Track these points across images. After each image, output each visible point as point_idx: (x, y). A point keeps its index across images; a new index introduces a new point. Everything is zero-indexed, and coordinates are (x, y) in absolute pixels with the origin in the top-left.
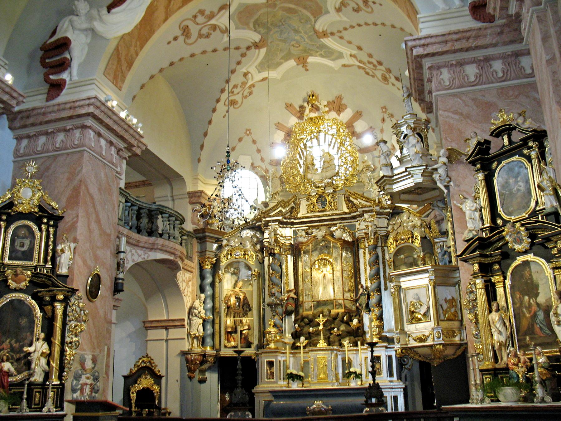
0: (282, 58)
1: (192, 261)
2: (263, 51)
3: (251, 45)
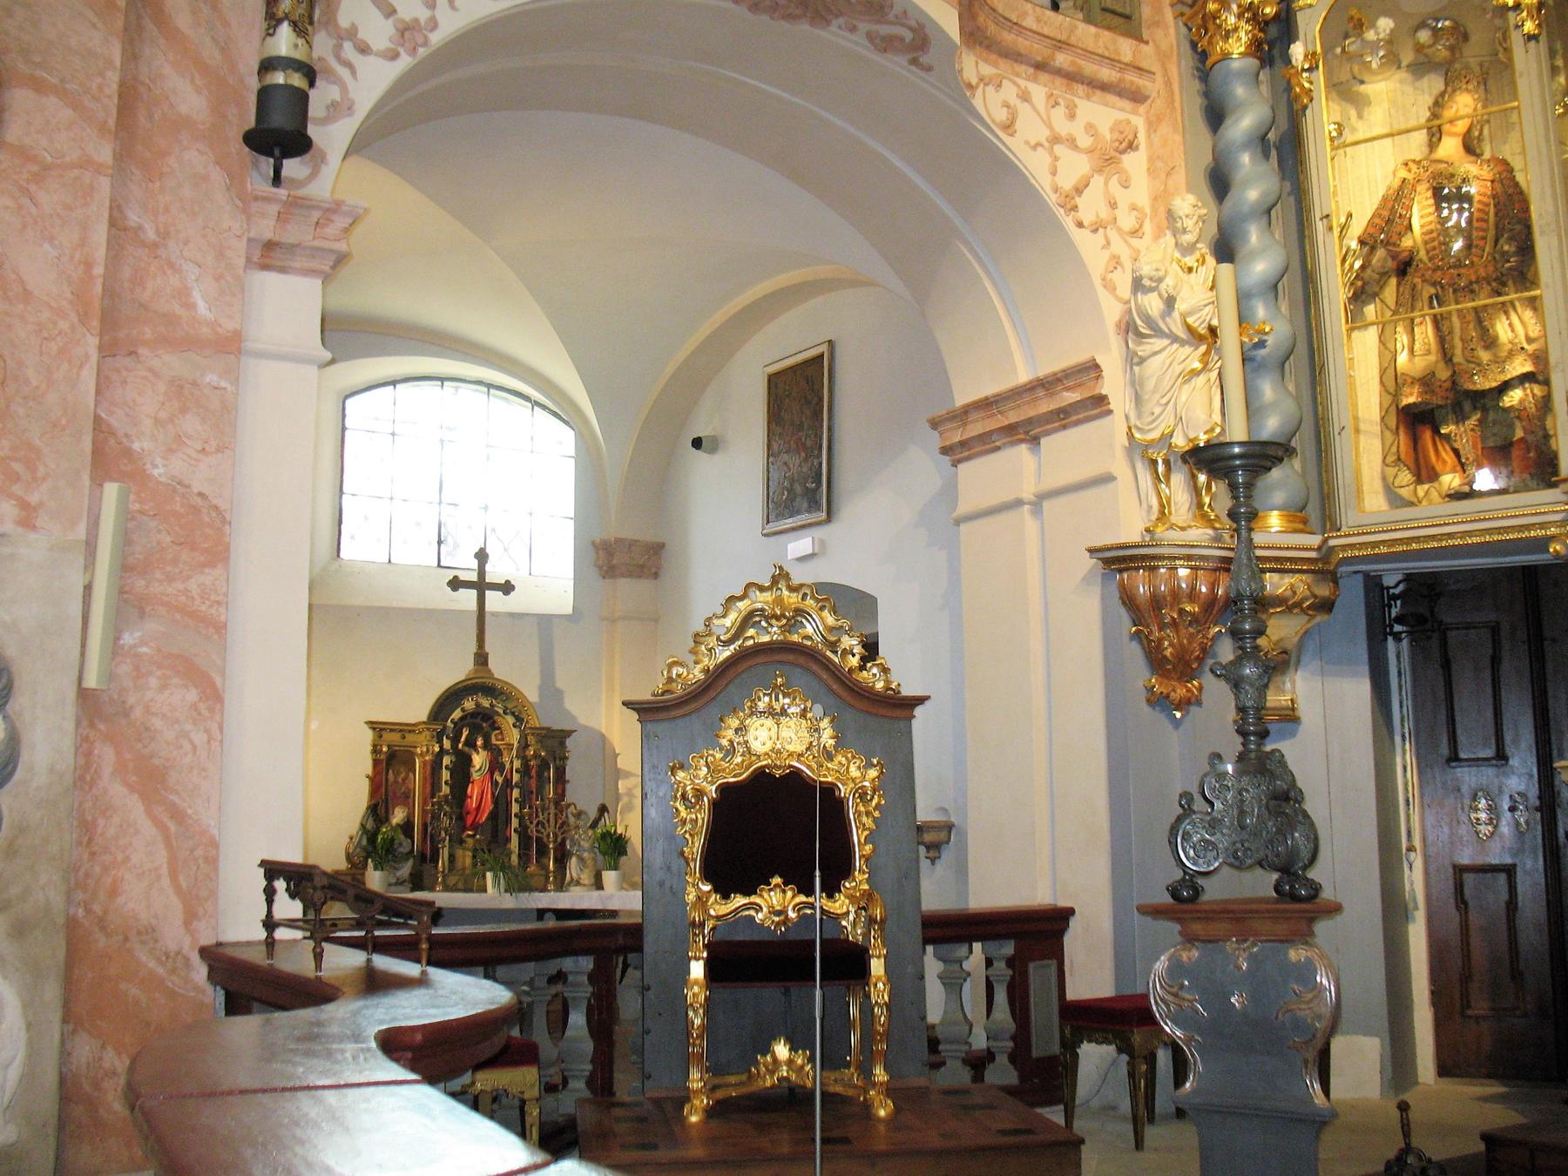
1: (1139, 39)
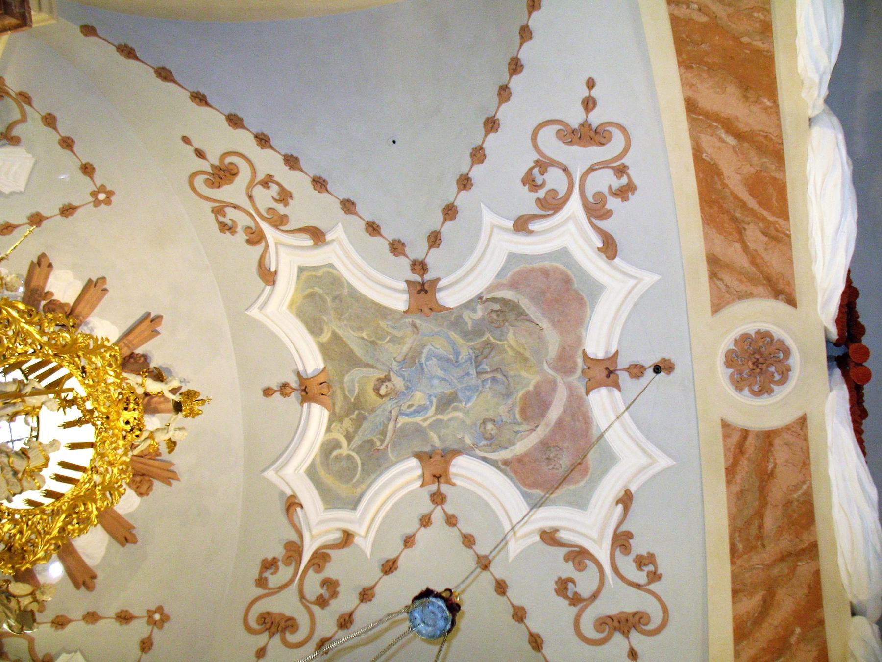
0: (335, 337)
2: (399, 302)
3: (427, 277)
